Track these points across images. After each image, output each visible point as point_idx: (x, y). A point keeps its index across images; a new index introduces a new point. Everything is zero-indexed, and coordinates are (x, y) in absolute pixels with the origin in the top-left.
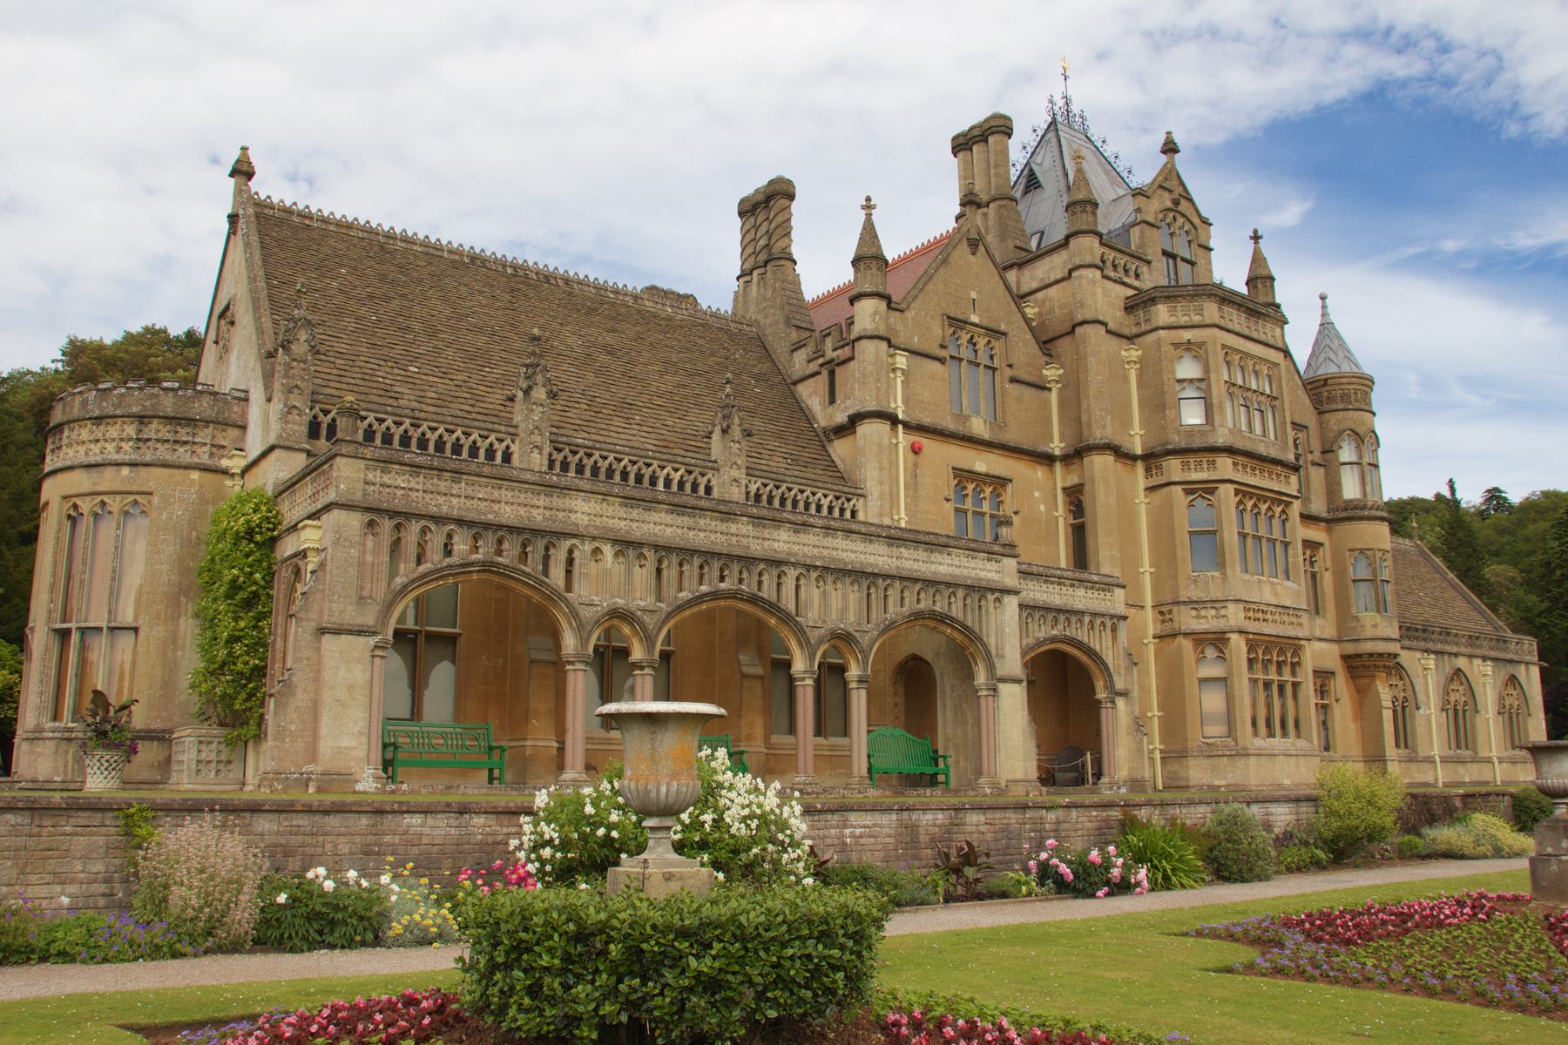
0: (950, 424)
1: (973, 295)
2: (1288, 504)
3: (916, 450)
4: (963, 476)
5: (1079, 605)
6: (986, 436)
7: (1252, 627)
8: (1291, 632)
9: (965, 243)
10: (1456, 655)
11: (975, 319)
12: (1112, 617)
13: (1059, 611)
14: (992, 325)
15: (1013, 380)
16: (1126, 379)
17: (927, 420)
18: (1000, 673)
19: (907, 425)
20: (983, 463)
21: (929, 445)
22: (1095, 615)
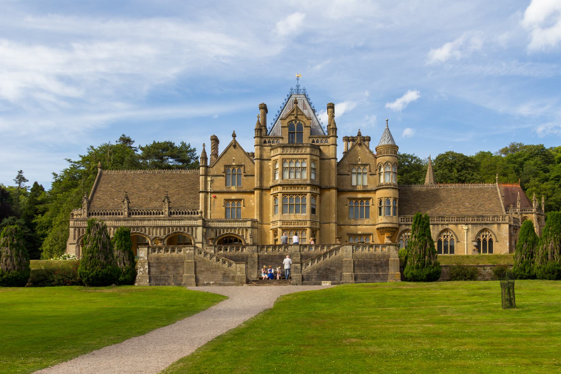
0: (225, 189)
1: (234, 158)
2: (306, 195)
3: (215, 197)
4: (227, 200)
5: (236, 226)
6: (236, 191)
7: (284, 226)
8: (303, 226)
9: (232, 147)
10: (447, 224)
11: (234, 164)
12: (246, 228)
13: (229, 228)
14: (239, 164)
15: (245, 176)
16: (270, 170)
17: (218, 190)
18: (196, 241)
19: (211, 192)
20: (233, 197)
21: (217, 195)
22: (240, 228)
